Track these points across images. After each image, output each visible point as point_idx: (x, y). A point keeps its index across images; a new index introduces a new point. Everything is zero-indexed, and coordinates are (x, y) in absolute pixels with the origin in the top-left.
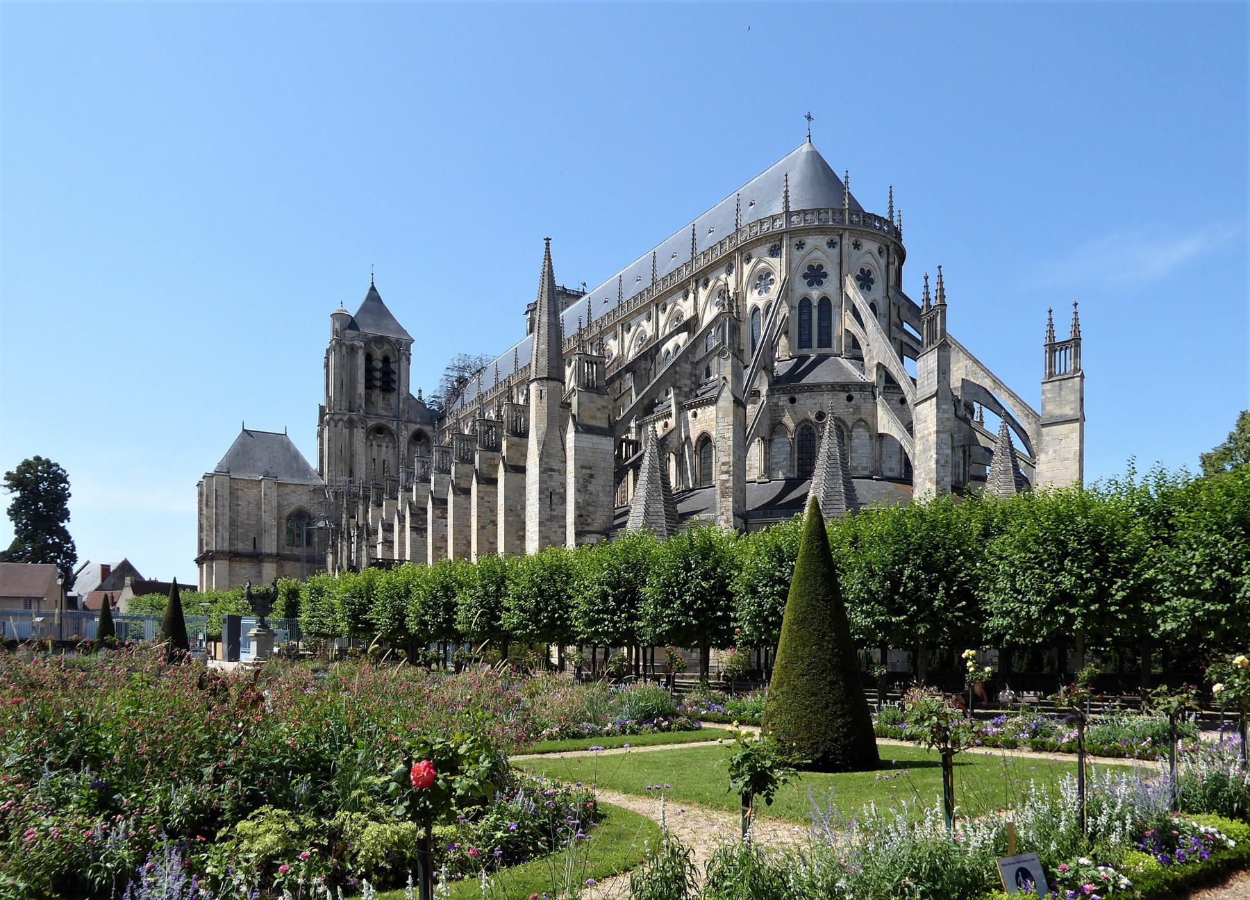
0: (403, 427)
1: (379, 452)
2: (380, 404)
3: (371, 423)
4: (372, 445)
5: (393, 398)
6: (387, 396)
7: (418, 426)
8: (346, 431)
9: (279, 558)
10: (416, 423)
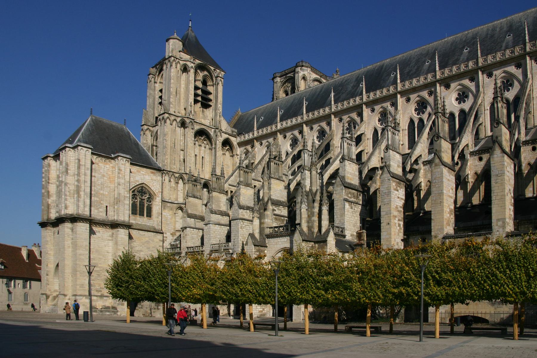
0: (219, 134)
1: (200, 150)
2: (201, 115)
3: (197, 127)
4: (195, 144)
5: (209, 113)
6: (205, 110)
7: (227, 136)
9: (128, 226)
10: (226, 133)
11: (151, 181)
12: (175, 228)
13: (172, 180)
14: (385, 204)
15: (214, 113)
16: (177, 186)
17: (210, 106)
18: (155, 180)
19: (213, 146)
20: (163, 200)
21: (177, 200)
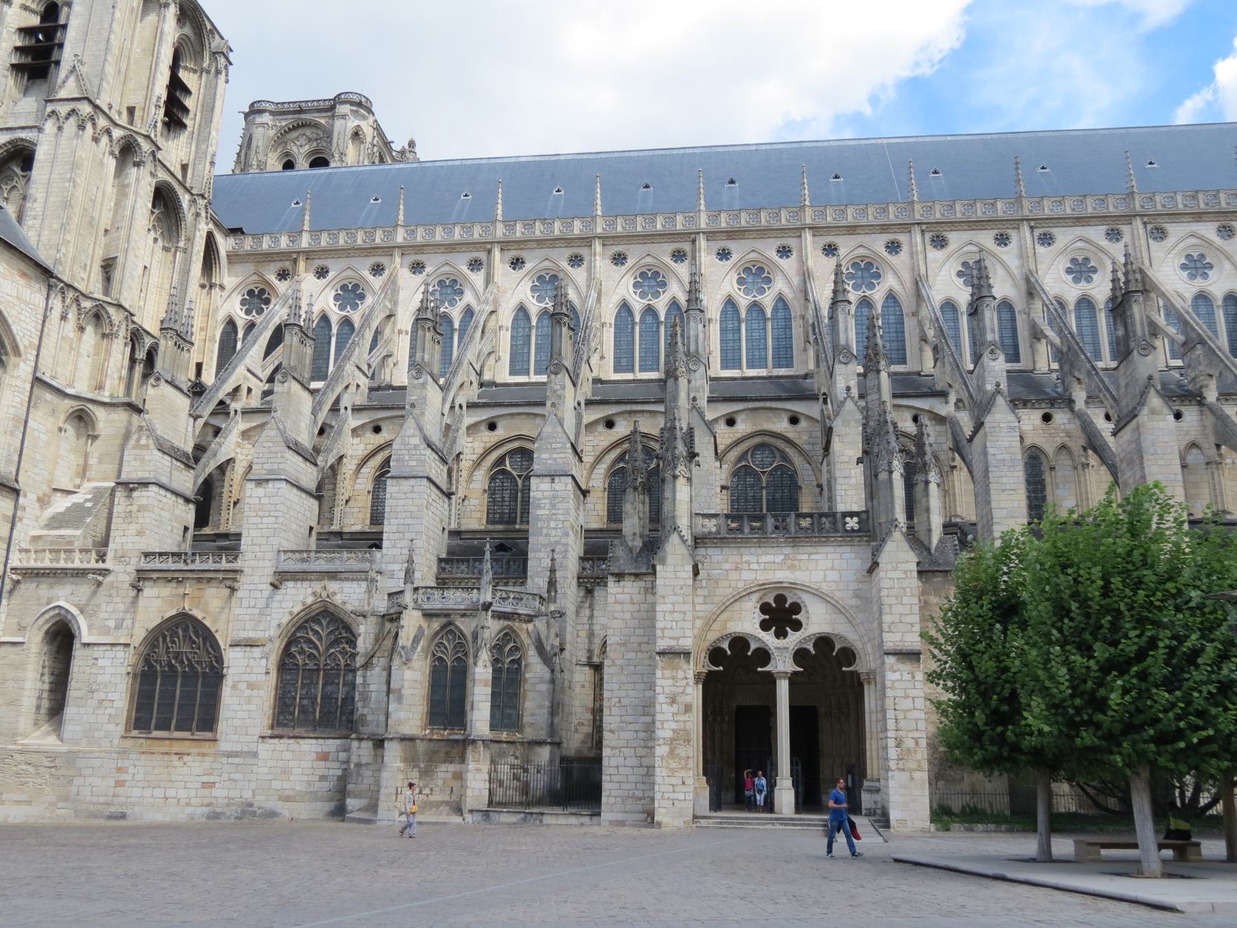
8: (111, 163)
11: (16, 302)
12: (51, 481)
13: (70, 316)
14: (1003, 491)
15: (193, 149)
16: (80, 339)
17: (184, 126)
18: (28, 304)
19: (181, 244)
20: (39, 375)
21: (71, 386)
